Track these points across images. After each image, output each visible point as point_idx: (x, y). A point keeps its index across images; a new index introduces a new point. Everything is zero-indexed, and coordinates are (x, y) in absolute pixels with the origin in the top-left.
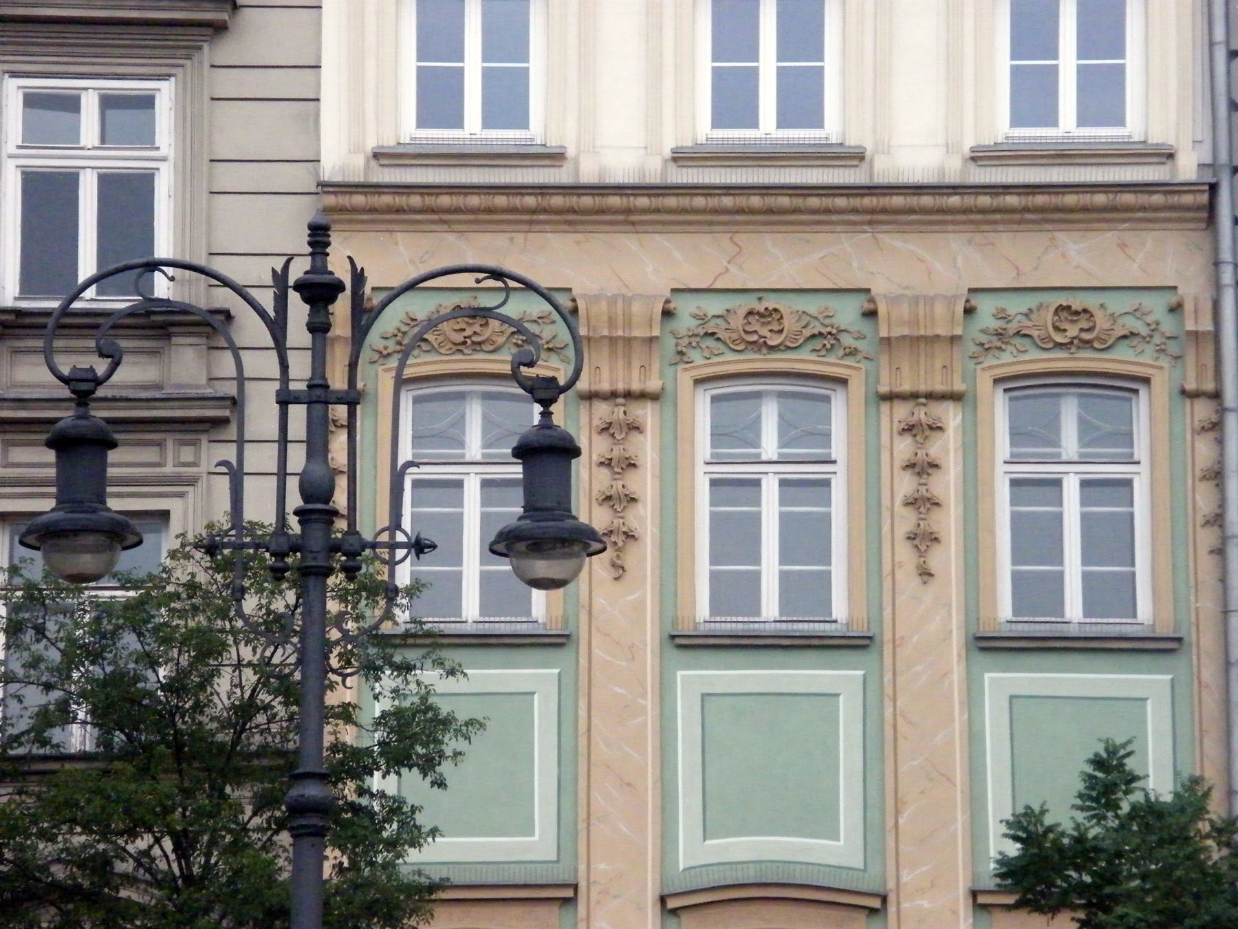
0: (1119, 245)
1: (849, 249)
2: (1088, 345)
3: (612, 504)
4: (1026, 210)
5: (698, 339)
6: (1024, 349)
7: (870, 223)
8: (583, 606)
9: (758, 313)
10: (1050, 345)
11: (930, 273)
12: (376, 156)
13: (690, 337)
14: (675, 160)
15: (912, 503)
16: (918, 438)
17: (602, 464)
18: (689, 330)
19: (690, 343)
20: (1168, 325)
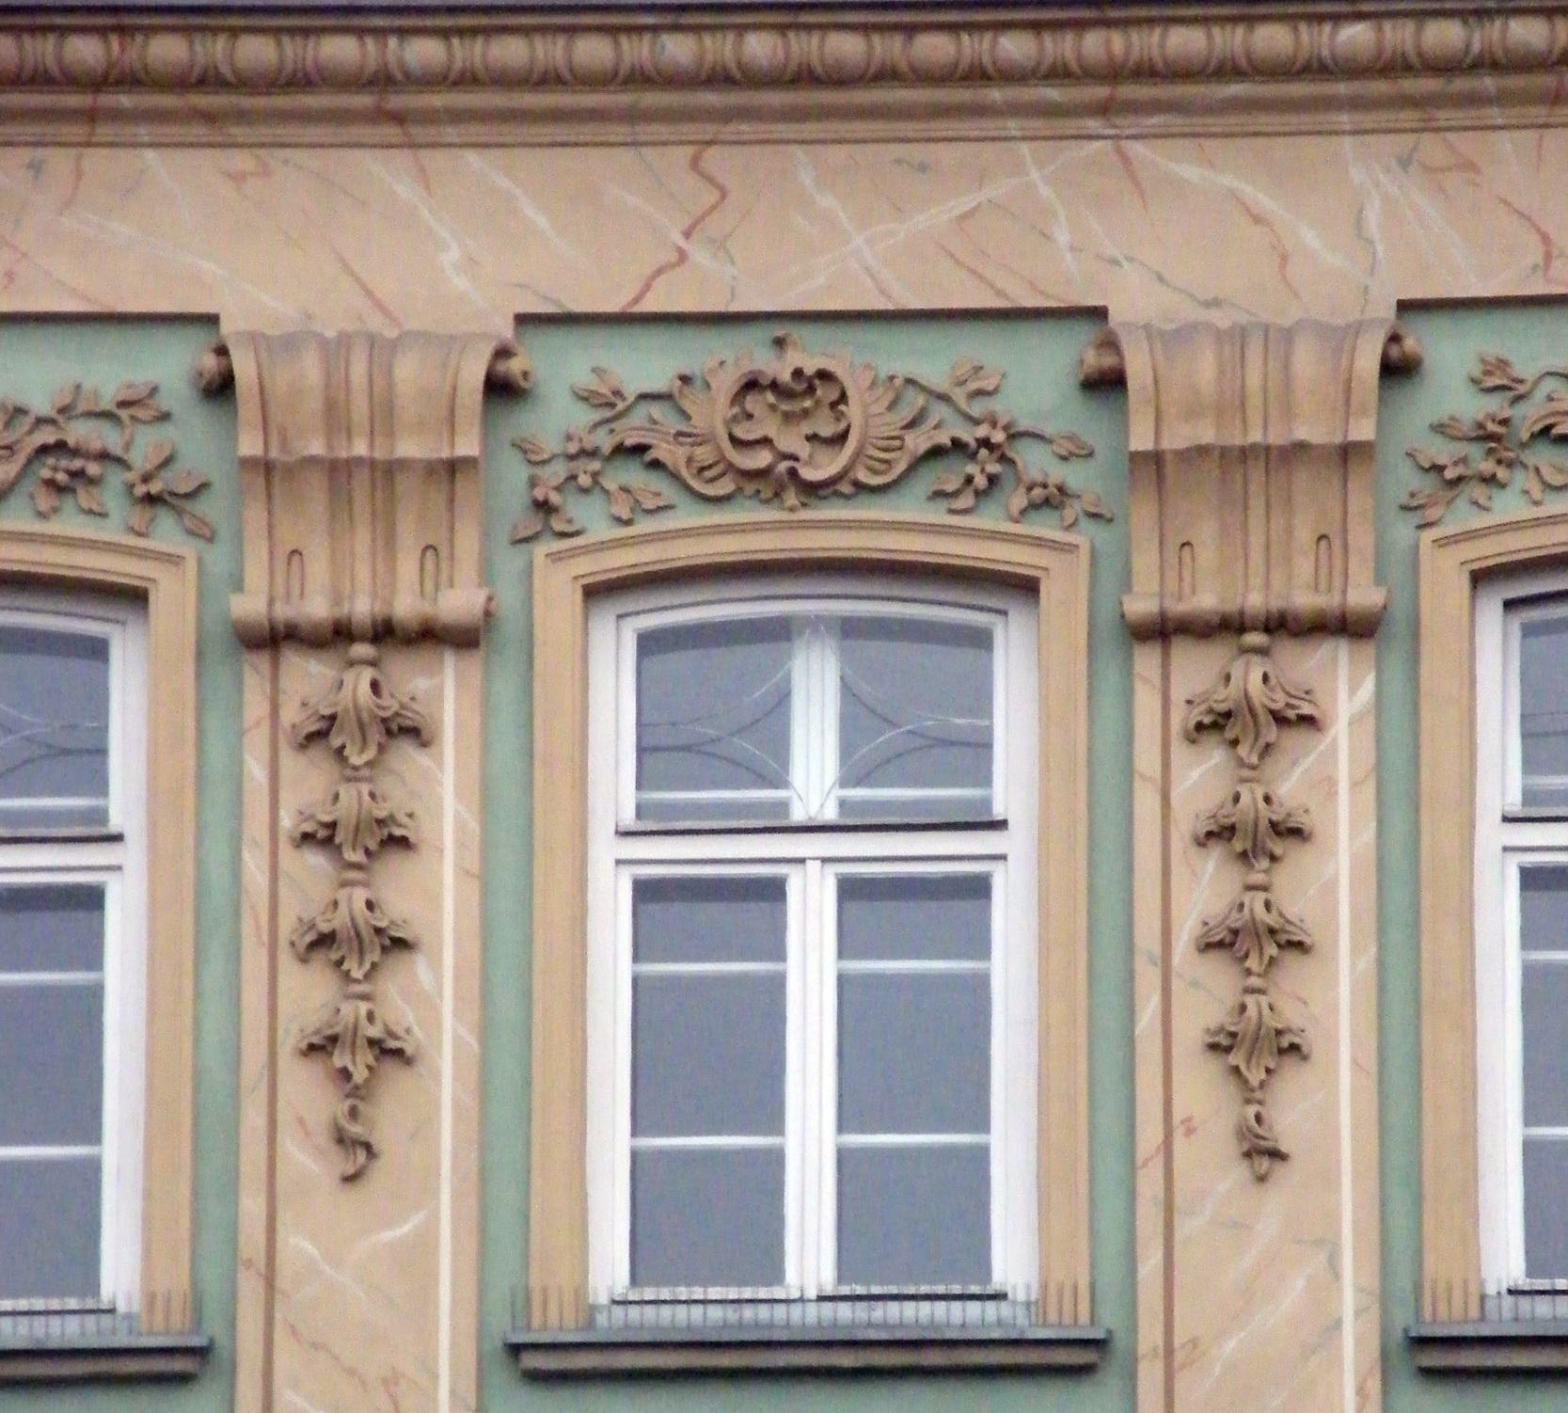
3: (335, 956)
5: (595, 465)
7: (1103, 109)
8: (249, 1263)
9: (774, 386)
11: (1284, 258)
13: (572, 458)
16: (1243, 750)
17: (307, 838)
18: (569, 438)
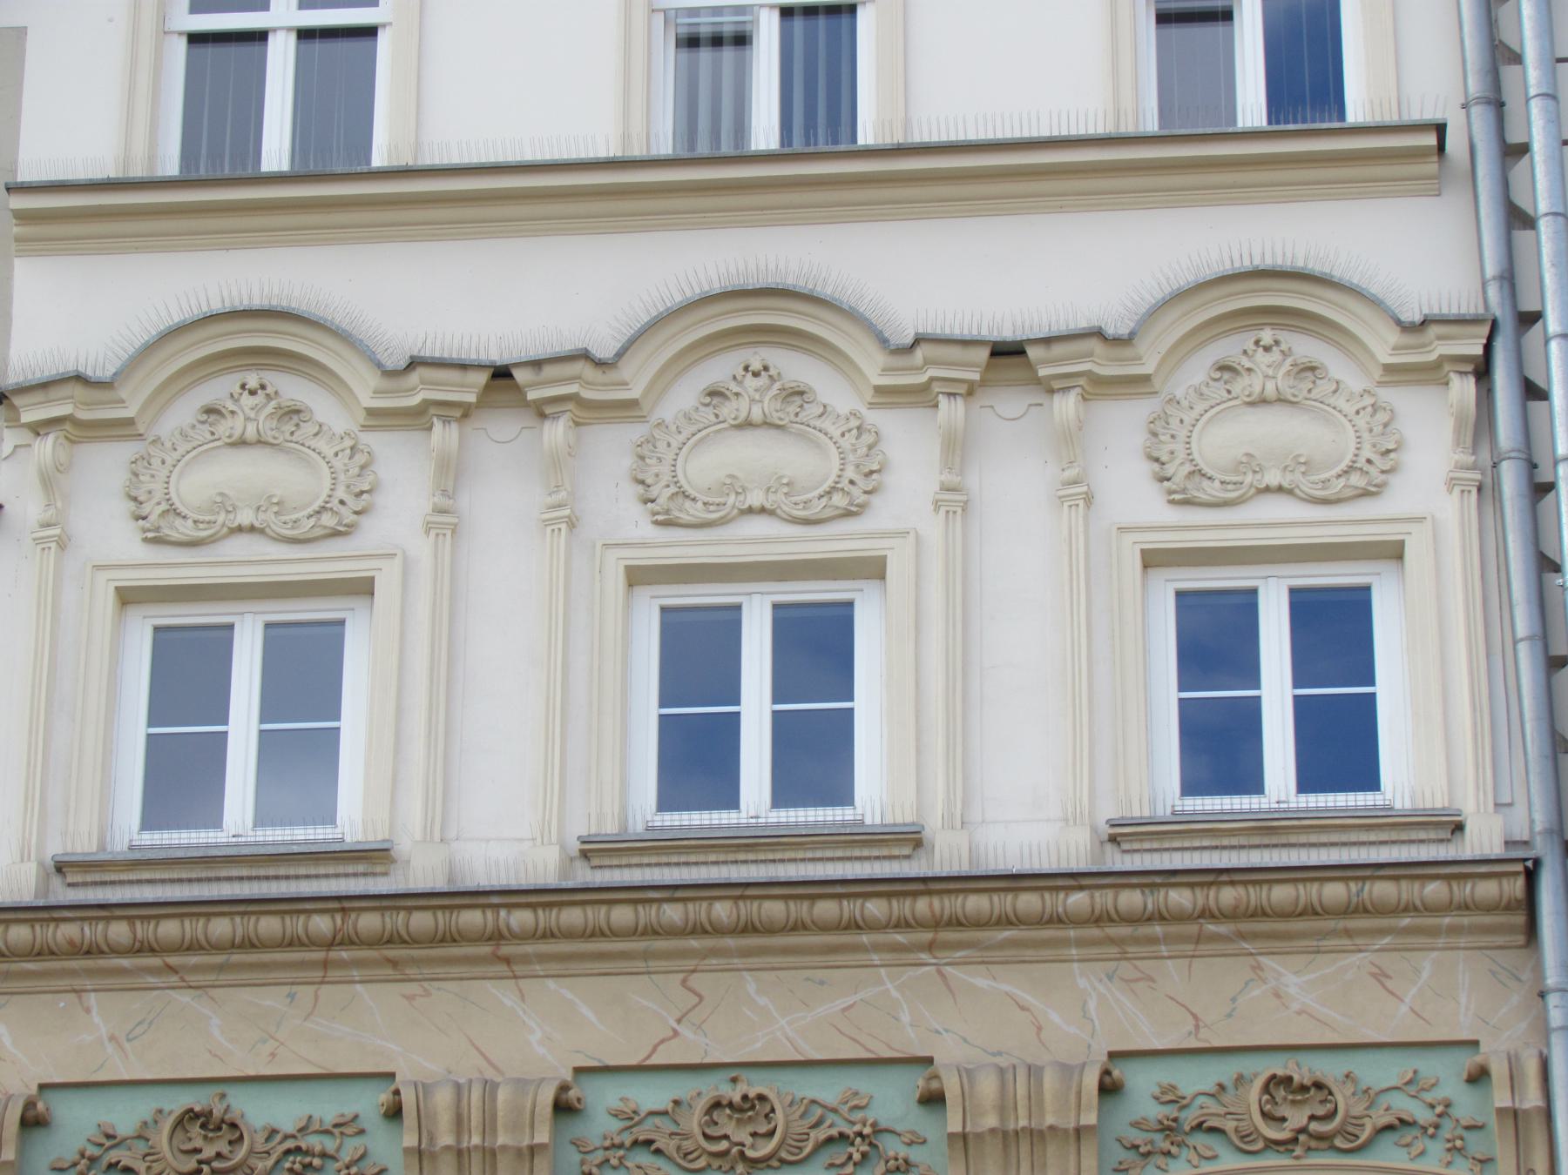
0: (1374, 975)
1: (895, 994)
2: (1323, 1145)
4: (1206, 914)
5: (621, 1152)
6: (1209, 1154)
7: (930, 947)
9: (731, 1105)
10: (1260, 1145)
11: (1040, 1029)
12: (60, 868)
13: (606, 1149)
14: (585, 854)
18: (605, 1138)
19: (607, 1161)
20: (1466, 1105)
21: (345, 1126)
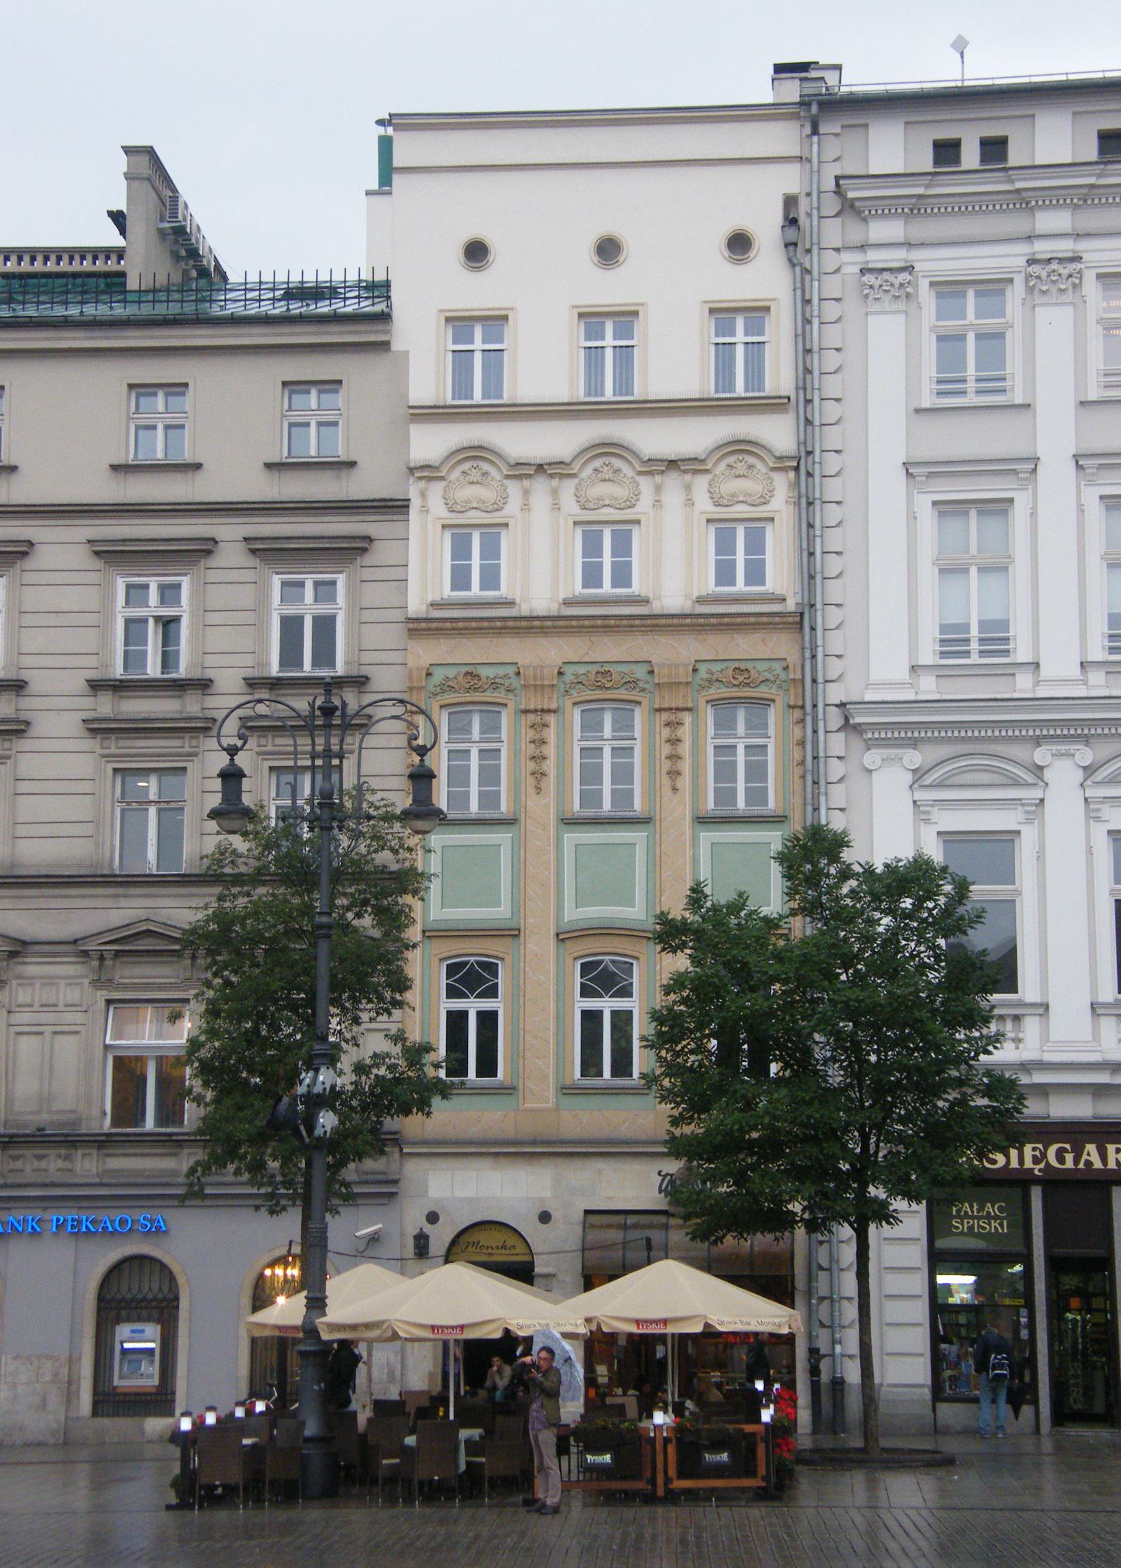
7: (651, 631)
12: (432, 605)
15: (669, 757)
20: (783, 676)
21: (506, 676)
